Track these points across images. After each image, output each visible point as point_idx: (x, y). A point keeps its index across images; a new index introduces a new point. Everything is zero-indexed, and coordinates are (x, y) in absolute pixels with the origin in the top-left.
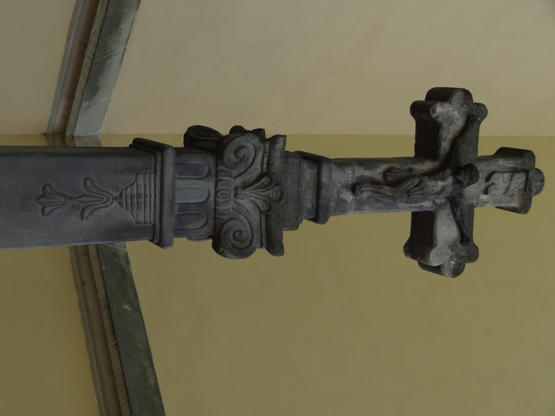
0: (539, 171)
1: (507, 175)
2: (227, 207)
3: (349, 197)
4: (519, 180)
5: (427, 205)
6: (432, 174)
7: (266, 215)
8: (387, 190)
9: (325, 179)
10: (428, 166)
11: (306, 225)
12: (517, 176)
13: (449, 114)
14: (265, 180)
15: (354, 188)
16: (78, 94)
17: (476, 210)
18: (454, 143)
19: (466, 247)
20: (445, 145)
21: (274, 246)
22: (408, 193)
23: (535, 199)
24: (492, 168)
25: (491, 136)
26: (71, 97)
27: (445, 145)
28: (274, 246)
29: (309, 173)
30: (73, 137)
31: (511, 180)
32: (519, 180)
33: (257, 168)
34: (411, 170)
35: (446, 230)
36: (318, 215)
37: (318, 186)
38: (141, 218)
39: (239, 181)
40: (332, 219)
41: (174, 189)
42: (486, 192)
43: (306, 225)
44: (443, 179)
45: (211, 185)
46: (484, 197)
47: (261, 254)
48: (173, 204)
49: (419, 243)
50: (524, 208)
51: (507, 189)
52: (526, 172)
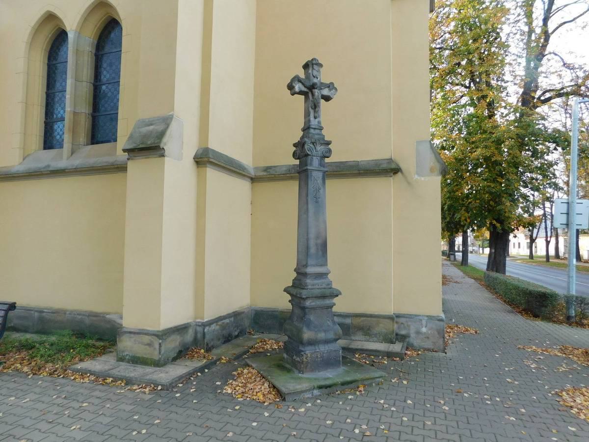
0: (312, 60)
1: (314, 71)
2: (320, 153)
3: (317, 120)
4: (315, 67)
5: (320, 97)
6: (313, 95)
7: (322, 144)
8: (316, 110)
9: (314, 127)
10: (310, 95)
11: (323, 132)
12: (314, 68)
13: (298, 87)
14: (315, 144)
15: (315, 118)
16: (244, 173)
17: (322, 81)
18: (305, 87)
19: (330, 86)
20: (305, 90)
21: (328, 143)
22: (318, 103)
23: (320, 62)
24: (311, 75)
25: (302, 74)
26: (244, 176)
27: (305, 90)
28: (328, 143)
29: (312, 131)
30: (255, 176)
31: (315, 70)
32: (315, 67)
33: (312, 145)
34: (312, 101)
35: (326, 92)
36: (321, 129)
37: (315, 129)
38: (321, 175)
39: (314, 150)
40: (323, 125)
41: (315, 167)
42: (317, 78)
43: (323, 132)
44: (315, 92)
45: (314, 158)
46: (319, 79)
47: (330, 146)
48: (317, 167)
49: (327, 98)
50: (321, 65)
51: (317, 71)
52: (313, 64)
